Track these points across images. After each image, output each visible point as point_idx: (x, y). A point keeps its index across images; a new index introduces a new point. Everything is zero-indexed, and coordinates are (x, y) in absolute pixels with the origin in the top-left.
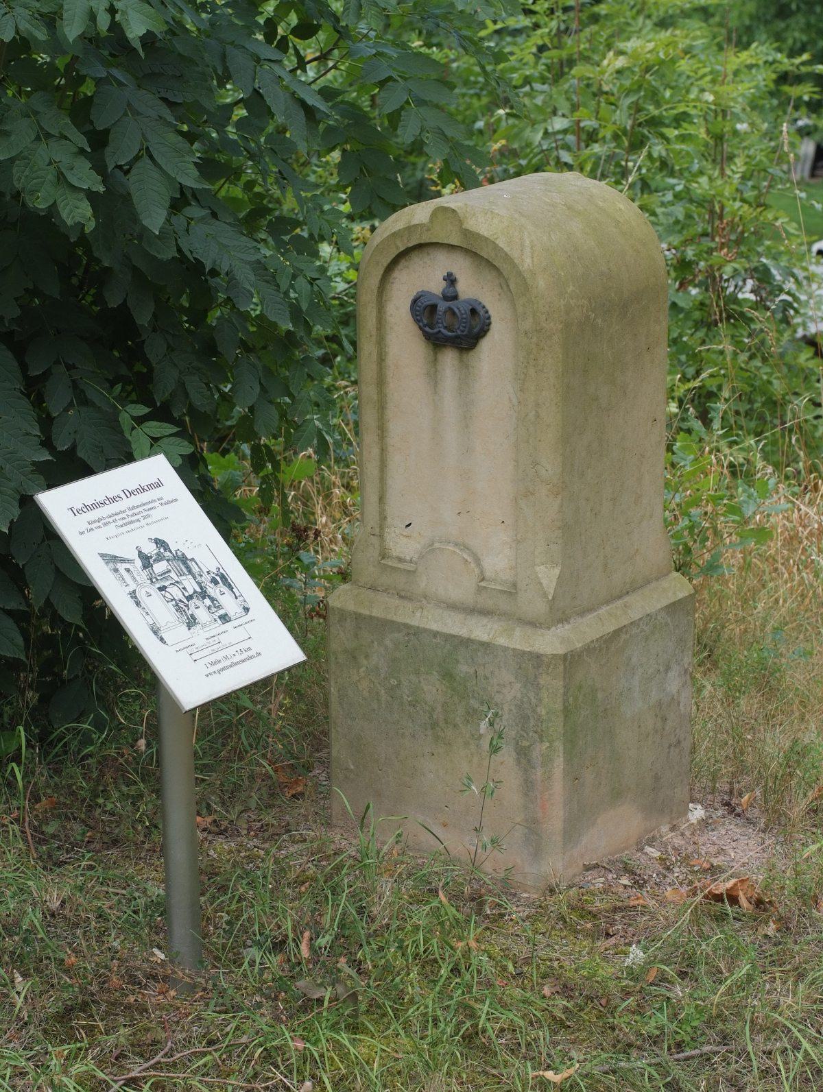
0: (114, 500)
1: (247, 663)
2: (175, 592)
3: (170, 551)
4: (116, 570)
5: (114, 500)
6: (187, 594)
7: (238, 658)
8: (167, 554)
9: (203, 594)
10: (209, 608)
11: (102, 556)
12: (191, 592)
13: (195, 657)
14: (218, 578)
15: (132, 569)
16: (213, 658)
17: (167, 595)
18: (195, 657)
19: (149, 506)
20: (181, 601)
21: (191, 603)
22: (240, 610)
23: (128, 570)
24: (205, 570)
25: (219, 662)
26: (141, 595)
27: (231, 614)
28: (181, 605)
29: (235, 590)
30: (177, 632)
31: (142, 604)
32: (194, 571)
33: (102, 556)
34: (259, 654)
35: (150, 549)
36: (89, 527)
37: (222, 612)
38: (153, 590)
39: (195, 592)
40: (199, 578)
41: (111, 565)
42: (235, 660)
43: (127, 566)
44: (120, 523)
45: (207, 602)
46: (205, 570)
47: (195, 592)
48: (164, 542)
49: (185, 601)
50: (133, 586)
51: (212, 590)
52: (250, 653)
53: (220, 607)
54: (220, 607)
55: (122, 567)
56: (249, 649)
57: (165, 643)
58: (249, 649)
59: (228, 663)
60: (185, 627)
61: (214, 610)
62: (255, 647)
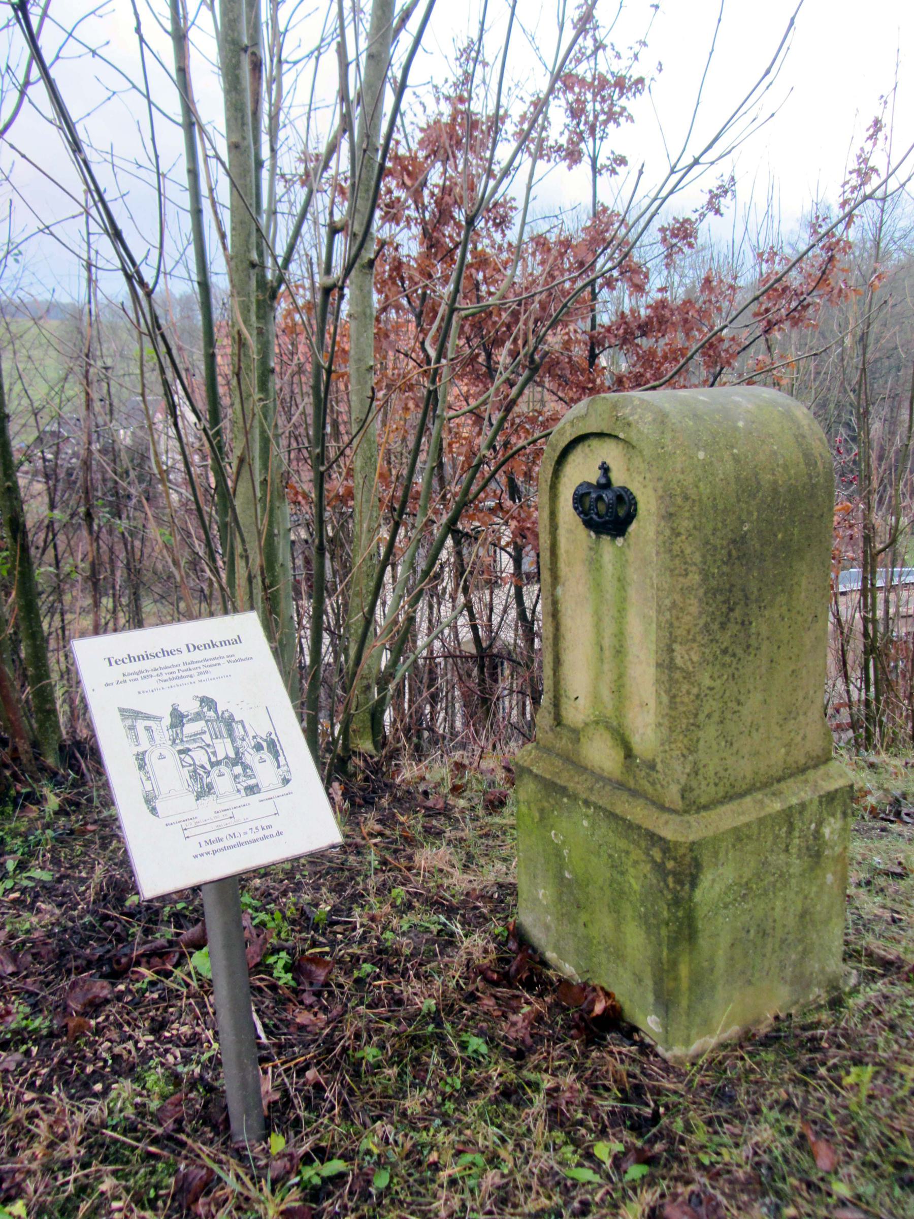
0: (170, 653)
1: (261, 843)
2: (200, 757)
3: (216, 711)
4: (132, 728)
5: (170, 653)
6: (213, 759)
7: (251, 836)
8: (211, 714)
9: (238, 760)
10: (236, 777)
11: (122, 710)
12: (221, 756)
13: (187, 833)
14: (265, 744)
15: (154, 727)
16: (207, 837)
17: (188, 759)
18: (187, 833)
19: (215, 662)
20: (203, 767)
21: (215, 771)
22: (277, 781)
23: (148, 729)
24: (251, 734)
25: (221, 840)
26: (152, 759)
27: (264, 785)
28: (200, 771)
29: (281, 758)
30: (177, 797)
31: (148, 768)
32: (237, 734)
33: (122, 710)
34: (279, 834)
35: (189, 706)
36: (121, 678)
37: (252, 782)
38: (170, 753)
39: (227, 757)
40: (239, 742)
41: (129, 722)
42: (243, 839)
43: (148, 723)
44: (165, 677)
45: (238, 769)
46: (251, 734)
47: (227, 757)
48: (212, 701)
49: (208, 767)
50: (145, 745)
51: (251, 758)
52: (267, 832)
53: (252, 776)
54: (252, 776)
55: (140, 725)
56: (269, 827)
57: (154, 811)
58: (269, 827)
59: (233, 841)
60: (193, 797)
61: (242, 778)
62: (277, 824)
